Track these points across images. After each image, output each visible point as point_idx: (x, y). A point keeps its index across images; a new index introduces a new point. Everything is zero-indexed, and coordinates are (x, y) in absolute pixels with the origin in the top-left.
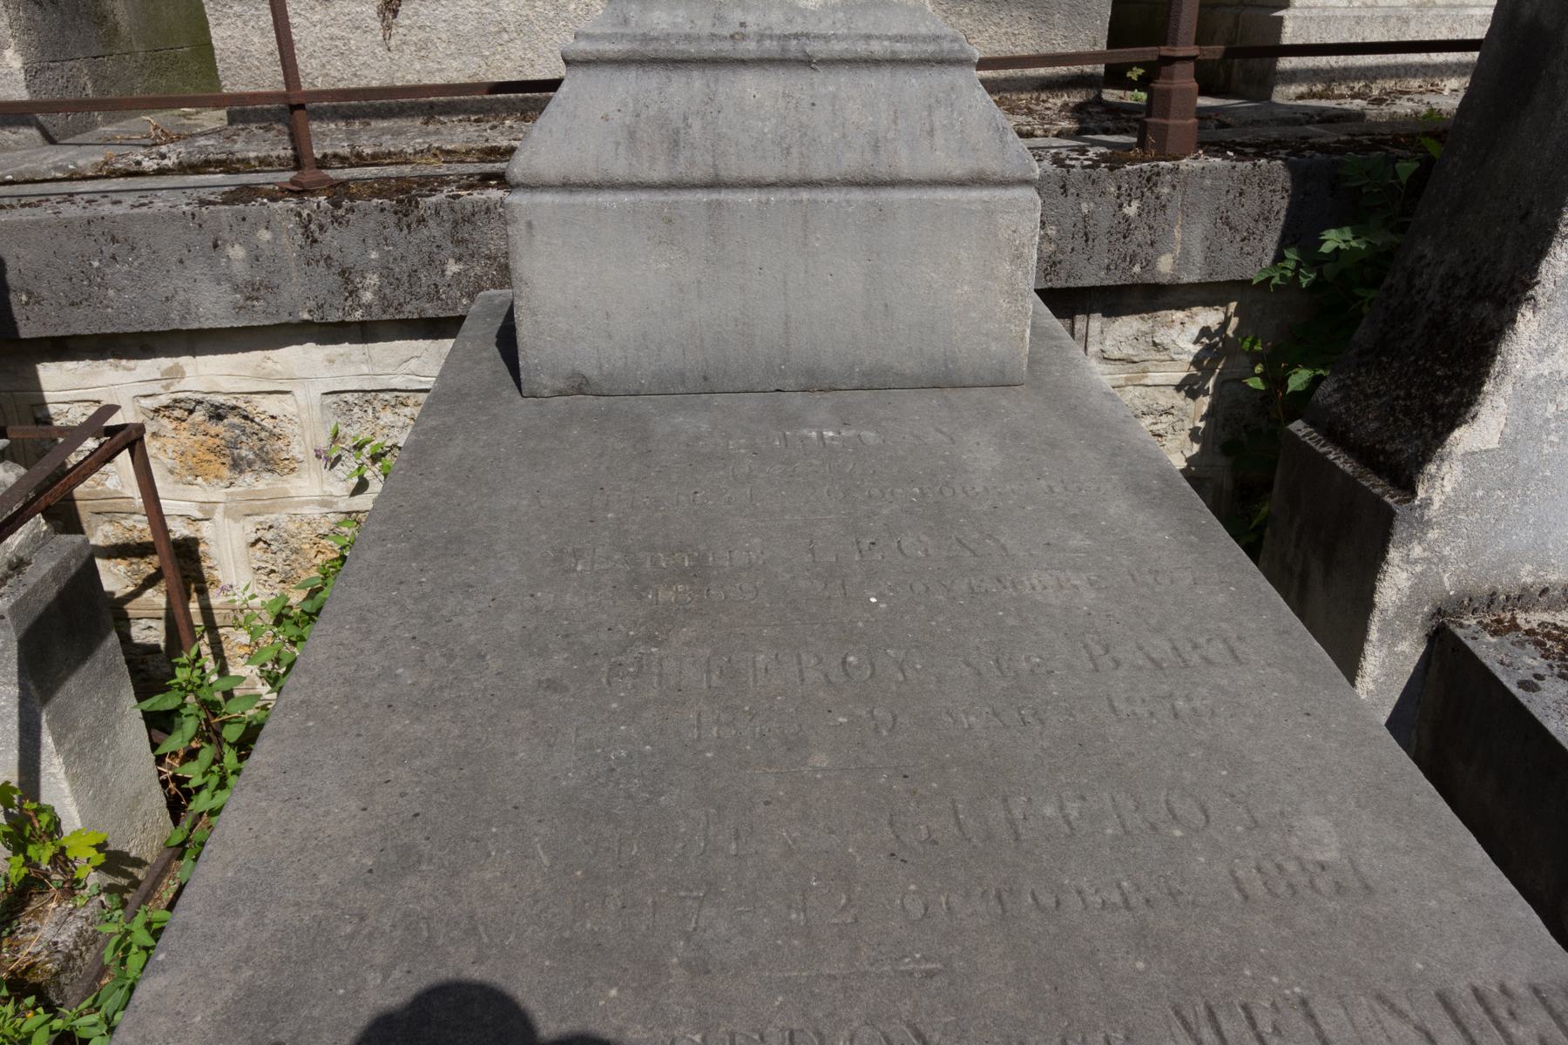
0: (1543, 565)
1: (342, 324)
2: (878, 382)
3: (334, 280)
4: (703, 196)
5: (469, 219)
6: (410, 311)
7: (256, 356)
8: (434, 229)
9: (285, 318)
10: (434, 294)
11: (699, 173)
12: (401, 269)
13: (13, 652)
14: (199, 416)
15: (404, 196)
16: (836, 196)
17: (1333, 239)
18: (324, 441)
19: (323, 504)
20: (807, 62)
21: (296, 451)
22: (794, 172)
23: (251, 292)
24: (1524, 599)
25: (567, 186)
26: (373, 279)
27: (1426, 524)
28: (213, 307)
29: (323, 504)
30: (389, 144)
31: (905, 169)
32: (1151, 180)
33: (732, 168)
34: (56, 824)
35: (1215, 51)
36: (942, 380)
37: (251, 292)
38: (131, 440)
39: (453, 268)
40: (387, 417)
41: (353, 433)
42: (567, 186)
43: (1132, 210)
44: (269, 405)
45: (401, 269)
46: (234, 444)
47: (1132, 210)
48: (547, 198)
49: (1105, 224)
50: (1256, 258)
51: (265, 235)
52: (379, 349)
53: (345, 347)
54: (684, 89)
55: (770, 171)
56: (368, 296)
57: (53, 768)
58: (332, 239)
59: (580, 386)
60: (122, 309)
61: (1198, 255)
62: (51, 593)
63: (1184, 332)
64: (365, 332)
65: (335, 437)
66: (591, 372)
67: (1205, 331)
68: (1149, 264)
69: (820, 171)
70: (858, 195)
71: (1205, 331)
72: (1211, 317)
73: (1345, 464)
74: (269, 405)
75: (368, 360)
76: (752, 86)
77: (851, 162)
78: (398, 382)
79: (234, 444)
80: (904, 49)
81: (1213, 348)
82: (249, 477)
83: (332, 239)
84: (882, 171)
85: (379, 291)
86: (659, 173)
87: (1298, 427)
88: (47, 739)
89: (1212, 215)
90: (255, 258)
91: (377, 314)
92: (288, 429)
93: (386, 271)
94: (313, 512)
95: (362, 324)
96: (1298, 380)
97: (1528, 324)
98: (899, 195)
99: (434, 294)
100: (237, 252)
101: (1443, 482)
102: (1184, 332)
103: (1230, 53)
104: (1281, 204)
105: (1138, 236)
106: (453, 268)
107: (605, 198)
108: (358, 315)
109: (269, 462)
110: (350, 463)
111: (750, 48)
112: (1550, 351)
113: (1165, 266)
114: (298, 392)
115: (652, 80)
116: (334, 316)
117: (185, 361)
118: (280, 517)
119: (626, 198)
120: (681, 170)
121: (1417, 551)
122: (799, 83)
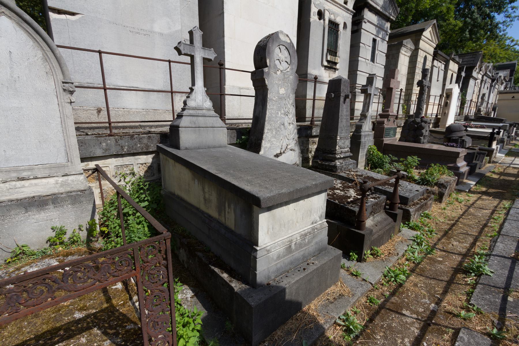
3: (120, 148)
6: (132, 152)
10: (136, 149)
12: (131, 146)
15: (132, 137)
18: (114, 174)
20: (205, 116)
25: (185, 127)
28: (99, 152)
30: (104, 132)
33: (200, 126)
36: (220, 147)
37: (106, 150)
39: (139, 145)
40: (125, 169)
42: (185, 127)
45: (131, 146)
51: (109, 141)
52: (125, 158)
53: (119, 158)
54: (194, 119)
56: (125, 150)
58: (120, 142)
64: (122, 156)
65: (116, 173)
76: (200, 118)
77: (211, 125)
78: (127, 163)
83: (120, 142)
86: (194, 126)
90: (107, 145)
91: (127, 152)
97: (263, 142)
99: (136, 149)
100: (104, 144)
106: (139, 145)
111: (200, 115)
114: (110, 166)
115: (191, 117)
120: (196, 126)
122: (205, 118)
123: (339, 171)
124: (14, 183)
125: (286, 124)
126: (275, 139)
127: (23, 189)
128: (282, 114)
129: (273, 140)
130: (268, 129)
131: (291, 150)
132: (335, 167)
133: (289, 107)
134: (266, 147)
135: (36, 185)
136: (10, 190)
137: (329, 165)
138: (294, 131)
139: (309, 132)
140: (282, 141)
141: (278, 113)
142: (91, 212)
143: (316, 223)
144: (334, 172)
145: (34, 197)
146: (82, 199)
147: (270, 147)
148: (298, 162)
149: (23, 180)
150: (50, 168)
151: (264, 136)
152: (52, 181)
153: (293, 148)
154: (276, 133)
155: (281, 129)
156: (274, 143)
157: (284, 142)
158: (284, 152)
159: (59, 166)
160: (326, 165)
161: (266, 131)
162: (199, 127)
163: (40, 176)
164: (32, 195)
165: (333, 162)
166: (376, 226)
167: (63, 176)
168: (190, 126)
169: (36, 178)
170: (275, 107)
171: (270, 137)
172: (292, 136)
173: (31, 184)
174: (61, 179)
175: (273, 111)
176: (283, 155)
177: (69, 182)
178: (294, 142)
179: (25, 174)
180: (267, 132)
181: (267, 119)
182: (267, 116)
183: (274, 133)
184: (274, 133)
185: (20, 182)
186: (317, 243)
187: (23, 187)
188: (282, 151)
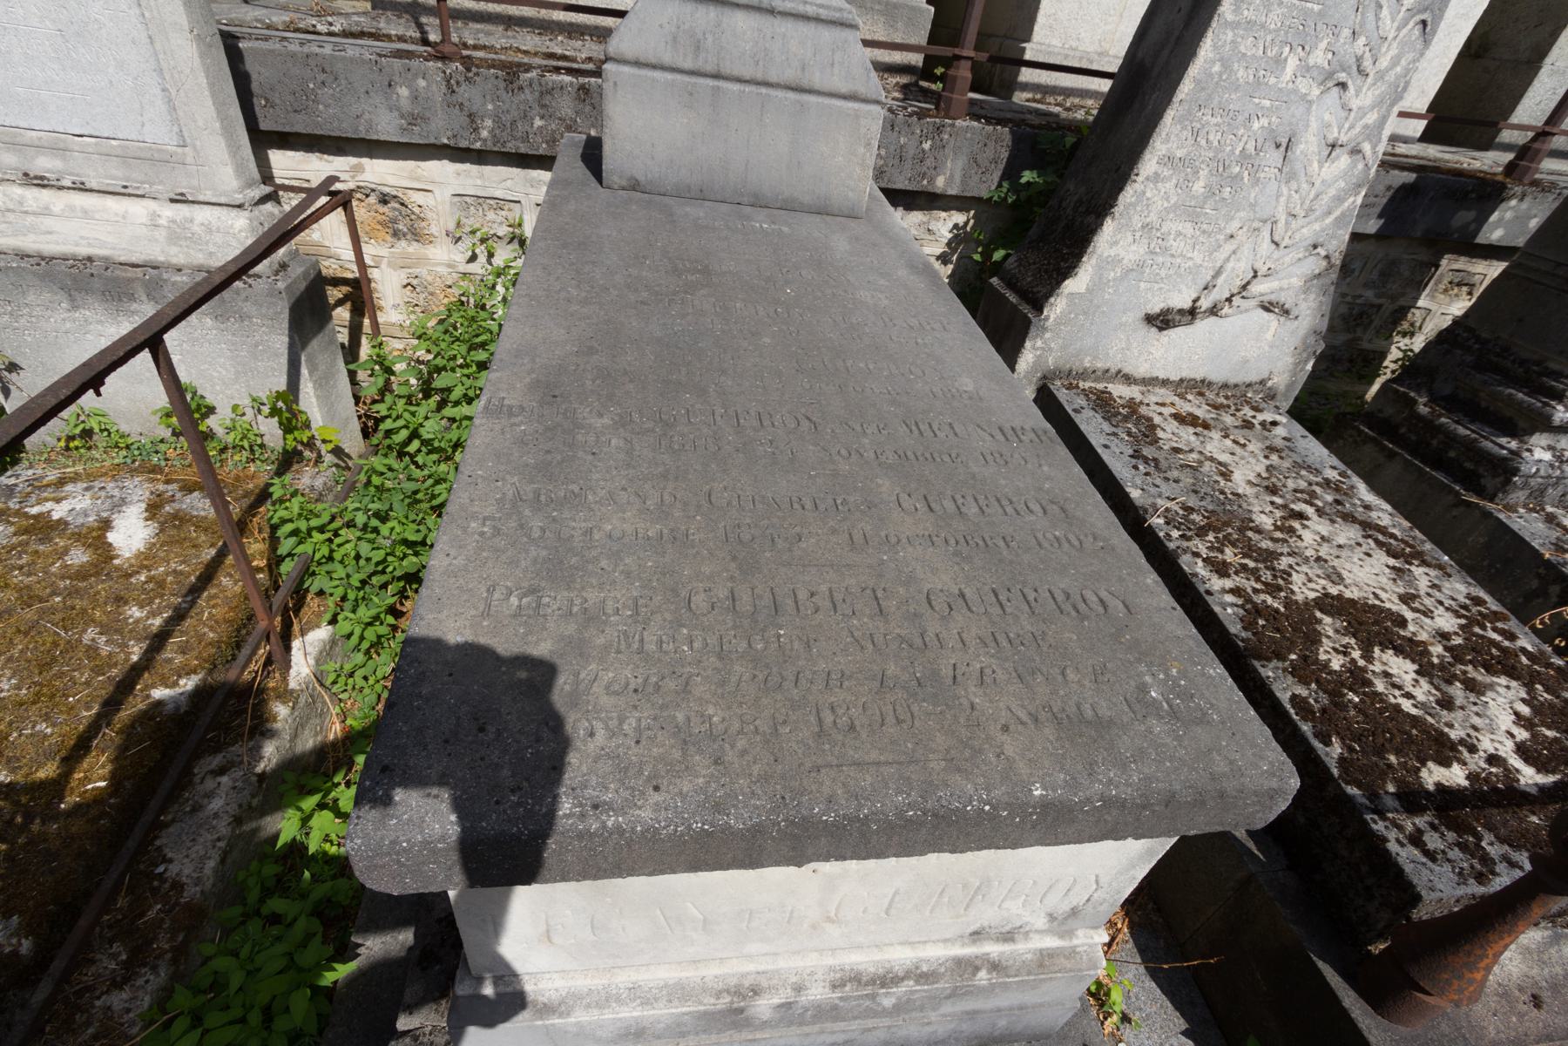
0: (1095, 358)
1: (468, 150)
2: (790, 207)
3: (465, 120)
4: (710, 82)
5: (550, 92)
6: (511, 147)
7: (411, 164)
8: (528, 95)
9: (432, 141)
10: (525, 138)
11: (709, 68)
12: (506, 119)
13: (286, 315)
14: (372, 199)
15: (512, 71)
16: (780, 94)
17: (1027, 176)
18: (451, 226)
19: (449, 266)
21: (434, 230)
22: (759, 76)
23: (413, 120)
24: (1084, 375)
25: (637, 63)
26: (489, 123)
27: (1045, 329)
28: (387, 127)
29: (449, 266)
30: (484, 40)
31: (817, 86)
32: (939, 129)
33: (727, 69)
34: (307, 425)
35: (983, 57)
36: (822, 210)
37: (413, 120)
38: (342, 201)
39: (538, 122)
40: (491, 215)
41: (470, 223)
42: (637, 63)
43: (927, 146)
44: (418, 198)
45: (506, 119)
46: (394, 221)
47: (927, 146)
48: (626, 69)
49: (912, 152)
50: (987, 185)
51: (422, 83)
52: (488, 170)
53: (467, 166)
55: (747, 73)
56: (485, 134)
57: (307, 388)
58: (464, 92)
59: (634, 186)
60: (327, 119)
61: (958, 179)
62: (303, 286)
63: (945, 224)
64: (480, 157)
65: (458, 225)
66: (641, 178)
67: (956, 226)
68: (932, 181)
69: (773, 79)
70: (791, 95)
71: (956, 226)
72: (960, 218)
73: (1013, 298)
74: (418, 198)
75: (482, 177)
77: (789, 75)
78: (498, 194)
79: (394, 221)
80: (823, 13)
81: (960, 238)
82: (403, 243)
83: (464, 92)
84: (805, 83)
85: (491, 131)
87: (994, 281)
88: (304, 371)
89: (967, 157)
90: (415, 98)
91: (490, 146)
92: (429, 215)
93: (497, 120)
94: (443, 270)
95: (479, 151)
96: (998, 255)
97: (1109, 226)
98: (812, 99)
99: (525, 138)
100: (404, 92)
101: (1056, 308)
102: (945, 224)
103: (992, 59)
104: (1005, 155)
105: (929, 162)
106: (538, 122)
107: (657, 74)
108: (478, 145)
109: (417, 235)
110: (467, 242)
112: (1116, 243)
113: (940, 183)
114: (436, 192)
116: (463, 144)
117: (365, 161)
118: (422, 271)
119: (669, 76)
120: (699, 64)
121: (1039, 343)
123: (1519, 496)
124: (17, 191)
125: (1309, 145)
126: (1188, 228)
127: (48, 222)
128: (1305, 69)
129: (1172, 226)
130: (1169, 160)
131: (1267, 307)
132: (1506, 469)
133: (1388, 25)
134: (1117, 261)
135: (86, 214)
136: (11, 217)
137: (1470, 447)
138: (1339, 199)
139: (1464, 217)
140: (1229, 247)
141: (1280, 62)
142: (284, 360)
143: (1008, 937)
144: (1480, 493)
145: (90, 259)
146: (248, 308)
147: (1141, 265)
148: (1279, 381)
149: (44, 186)
150: (125, 158)
151: (1127, 196)
152: (138, 210)
153: (1287, 299)
154: (1210, 192)
155: (1255, 169)
156: (1176, 245)
157: (1246, 251)
158: (1214, 311)
159: (155, 159)
160: (1452, 438)
161: (1149, 164)
162: (717, 76)
163: (93, 184)
164: (84, 251)
165: (1513, 434)
166: (1537, 1001)
167: (173, 201)
168: (667, 58)
169: (81, 188)
170: (1274, 19)
171: (1160, 204)
172: (1308, 231)
173: (72, 208)
174: (169, 212)
175: (1246, 46)
176: (1203, 326)
177: (196, 228)
178: (1315, 265)
179: (43, 164)
180: (1156, 178)
181: (1186, 88)
182: (1194, 70)
183: (1198, 187)
184: (1198, 187)
185: (36, 191)
186: (972, 1014)
187: (46, 212)
188: (1205, 304)
